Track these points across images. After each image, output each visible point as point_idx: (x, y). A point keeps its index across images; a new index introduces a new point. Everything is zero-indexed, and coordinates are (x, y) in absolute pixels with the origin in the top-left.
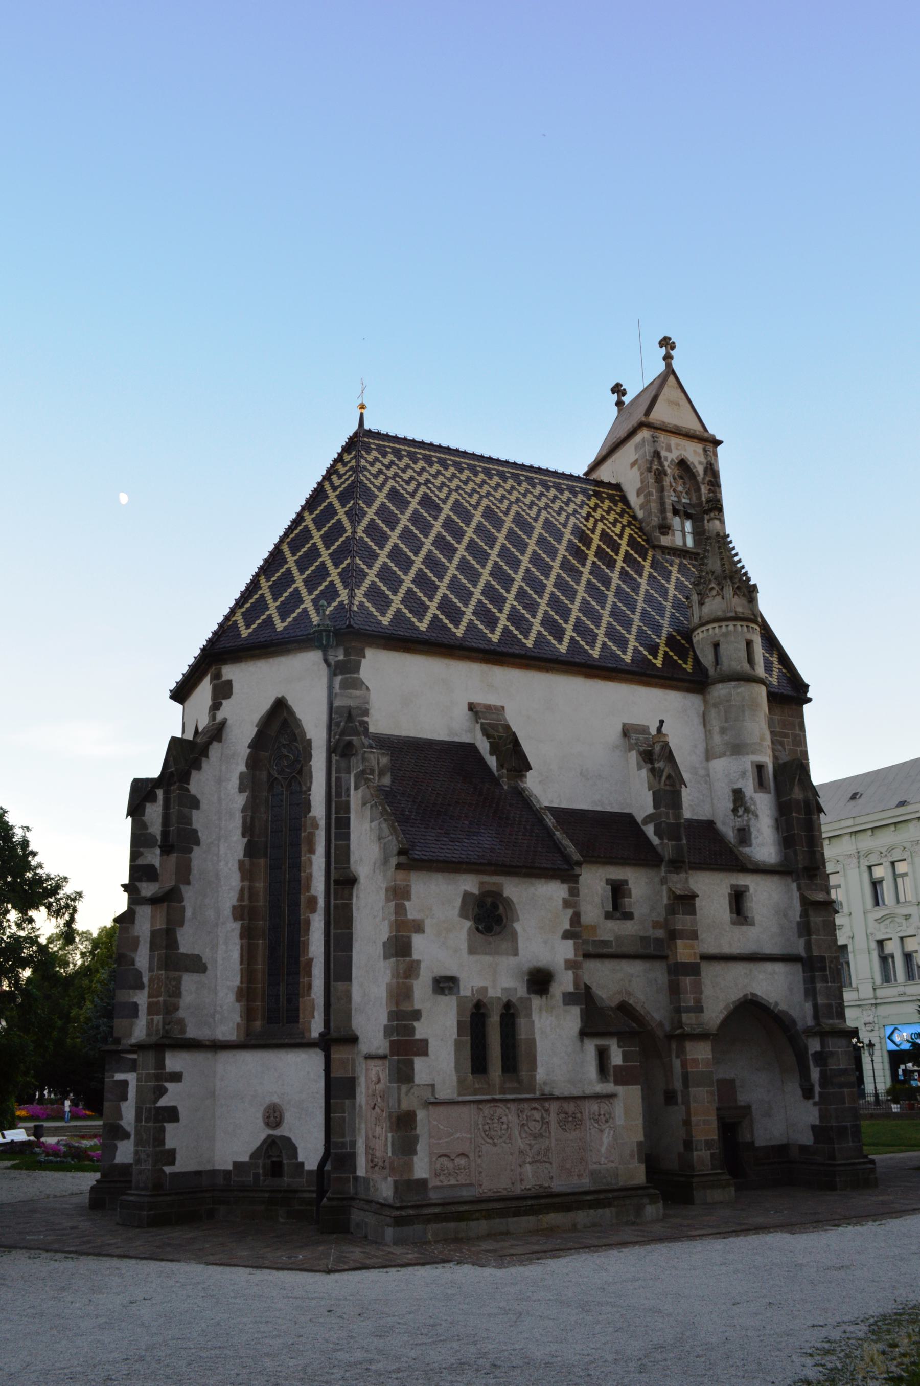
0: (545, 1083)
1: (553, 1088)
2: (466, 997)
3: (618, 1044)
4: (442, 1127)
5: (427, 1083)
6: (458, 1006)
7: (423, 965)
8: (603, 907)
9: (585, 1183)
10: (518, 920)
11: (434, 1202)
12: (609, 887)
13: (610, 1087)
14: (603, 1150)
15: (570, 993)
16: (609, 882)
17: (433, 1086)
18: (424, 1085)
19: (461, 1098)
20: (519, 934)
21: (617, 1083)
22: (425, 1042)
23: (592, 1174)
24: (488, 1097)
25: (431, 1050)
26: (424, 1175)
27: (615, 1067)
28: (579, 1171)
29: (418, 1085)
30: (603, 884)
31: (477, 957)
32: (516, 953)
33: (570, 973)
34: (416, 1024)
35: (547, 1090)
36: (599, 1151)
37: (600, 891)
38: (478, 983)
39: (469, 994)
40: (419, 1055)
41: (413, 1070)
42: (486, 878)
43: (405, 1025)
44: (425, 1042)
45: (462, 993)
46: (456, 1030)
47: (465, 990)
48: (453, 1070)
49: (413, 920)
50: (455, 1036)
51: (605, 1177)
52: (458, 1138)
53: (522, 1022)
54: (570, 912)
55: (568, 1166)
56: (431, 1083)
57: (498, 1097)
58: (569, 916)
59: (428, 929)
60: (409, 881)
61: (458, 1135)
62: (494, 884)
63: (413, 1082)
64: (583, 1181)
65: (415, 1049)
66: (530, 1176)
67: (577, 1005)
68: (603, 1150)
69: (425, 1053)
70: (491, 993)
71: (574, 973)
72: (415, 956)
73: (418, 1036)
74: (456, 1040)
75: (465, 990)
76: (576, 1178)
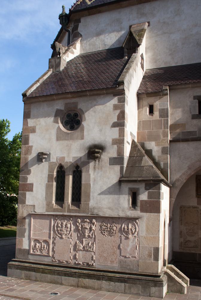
0: (94, 208)
1: (99, 211)
2: (53, 162)
3: (145, 188)
4: (37, 226)
5: (31, 204)
6: (49, 167)
7: (33, 148)
8: (191, 113)
9: (116, 267)
10: (85, 120)
11: (31, 261)
12: (197, 101)
13: (136, 213)
14: (129, 249)
15: (114, 158)
16: (195, 98)
17: (34, 206)
18: (29, 205)
19: (47, 213)
20: (85, 128)
21: (142, 211)
22: (32, 185)
23: (121, 262)
24: (61, 213)
25: (34, 189)
26: (27, 248)
27: (142, 201)
28: (112, 259)
29: (27, 205)
30: (191, 99)
31: (61, 142)
32: (82, 138)
33: (115, 147)
34: (28, 176)
35: (96, 211)
36: (126, 250)
37: (189, 104)
38: (59, 155)
39: (55, 161)
40: (29, 191)
41: (25, 198)
42: (68, 101)
43: (23, 177)
44: (32, 185)
45: (52, 160)
46: (47, 179)
47: (53, 159)
48: (45, 198)
49: (31, 127)
50: (47, 182)
51: (129, 266)
52: (44, 232)
53: (84, 175)
54: (118, 112)
55: (105, 255)
56: (33, 204)
57: (66, 214)
58: (117, 114)
59: (37, 130)
60: (30, 109)
61: (44, 231)
62: (73, 103)
63: (25, 204)
64: (114, 265)
65: (27, 188)
66: (82, 257)
67: (119, 165)
68: (129, 249)
69: (32, 190)
70: (67, 160)
71: (117, 146)
72: (30, 144)
73: (29, 182)
74: (47, 184)
75: (53, 159)
76: (109, 262)
